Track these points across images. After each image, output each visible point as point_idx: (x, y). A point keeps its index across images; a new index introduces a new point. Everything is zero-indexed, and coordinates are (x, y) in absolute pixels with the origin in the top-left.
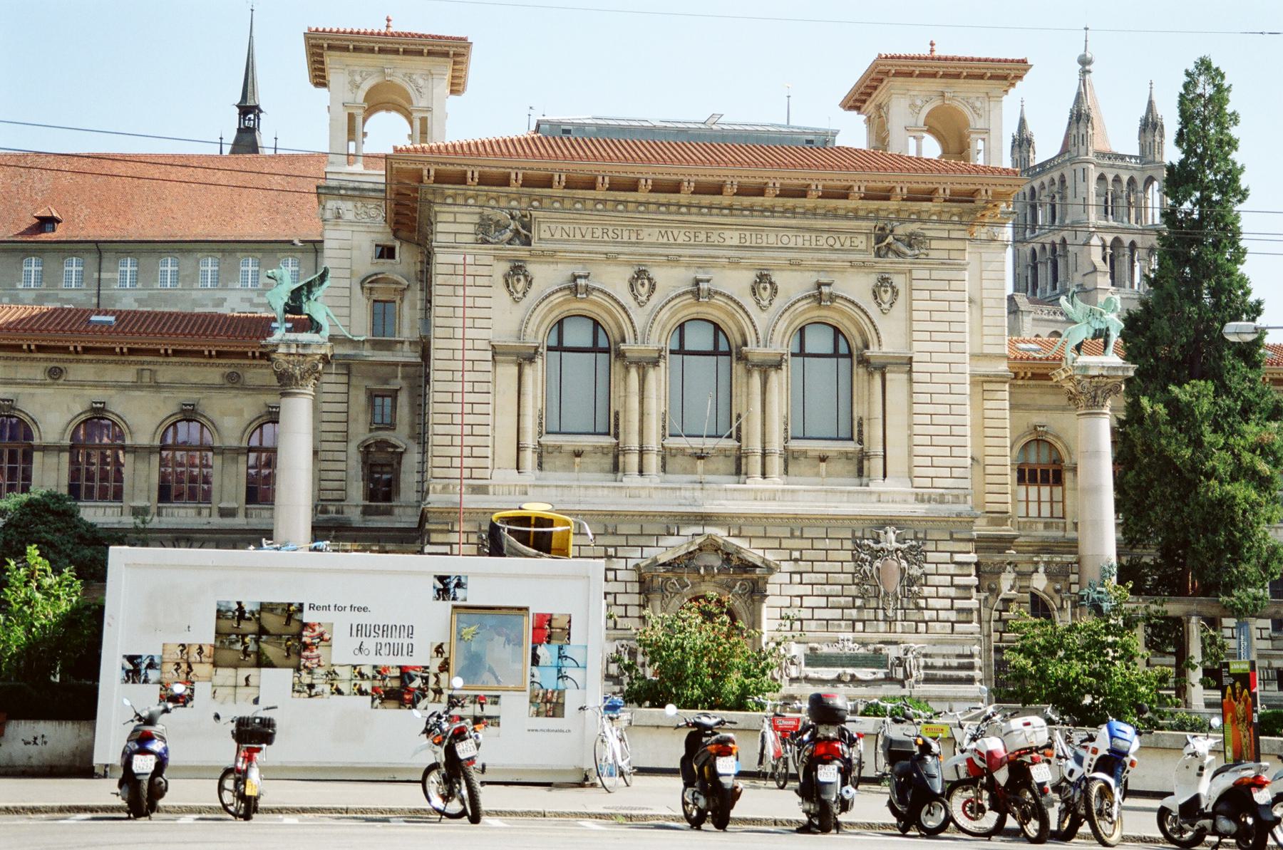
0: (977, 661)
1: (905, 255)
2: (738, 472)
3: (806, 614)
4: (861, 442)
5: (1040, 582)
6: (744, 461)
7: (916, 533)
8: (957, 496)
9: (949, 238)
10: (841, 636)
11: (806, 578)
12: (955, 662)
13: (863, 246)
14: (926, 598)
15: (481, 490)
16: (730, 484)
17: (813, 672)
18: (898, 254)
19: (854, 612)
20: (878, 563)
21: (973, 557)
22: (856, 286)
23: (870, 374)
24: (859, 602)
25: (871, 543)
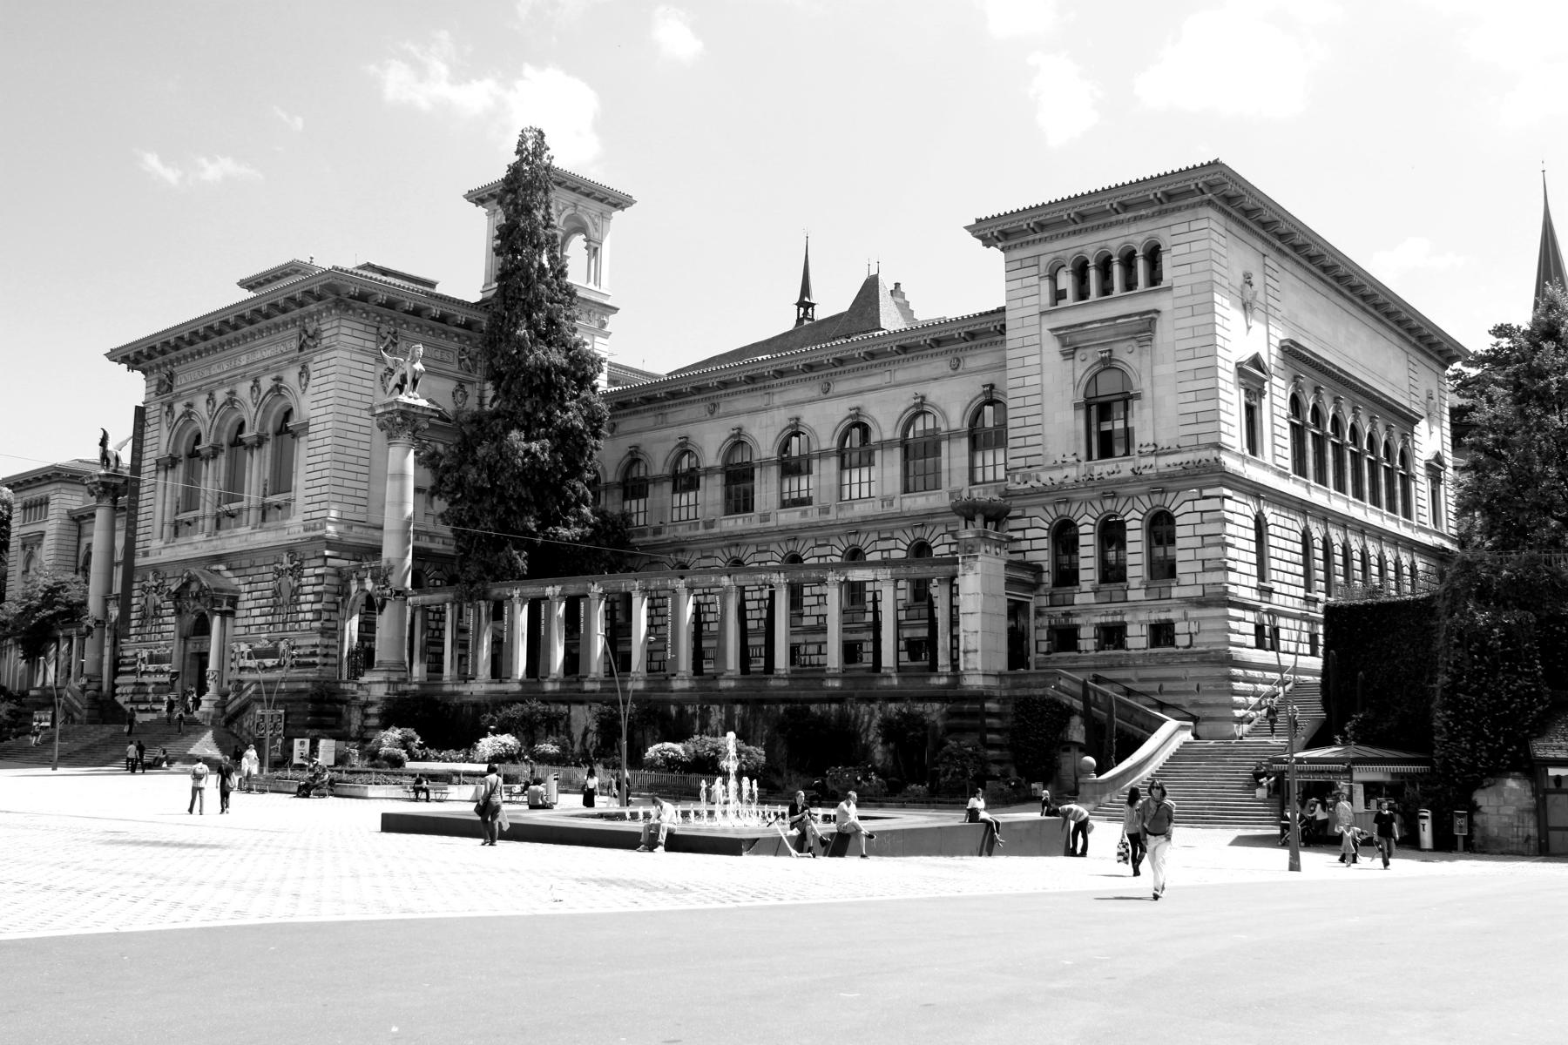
3: (251, 621)
5: (369, 585)
11: (255, 594)
12: (308, 651)
15: (146, 554)
17: (249, 663)
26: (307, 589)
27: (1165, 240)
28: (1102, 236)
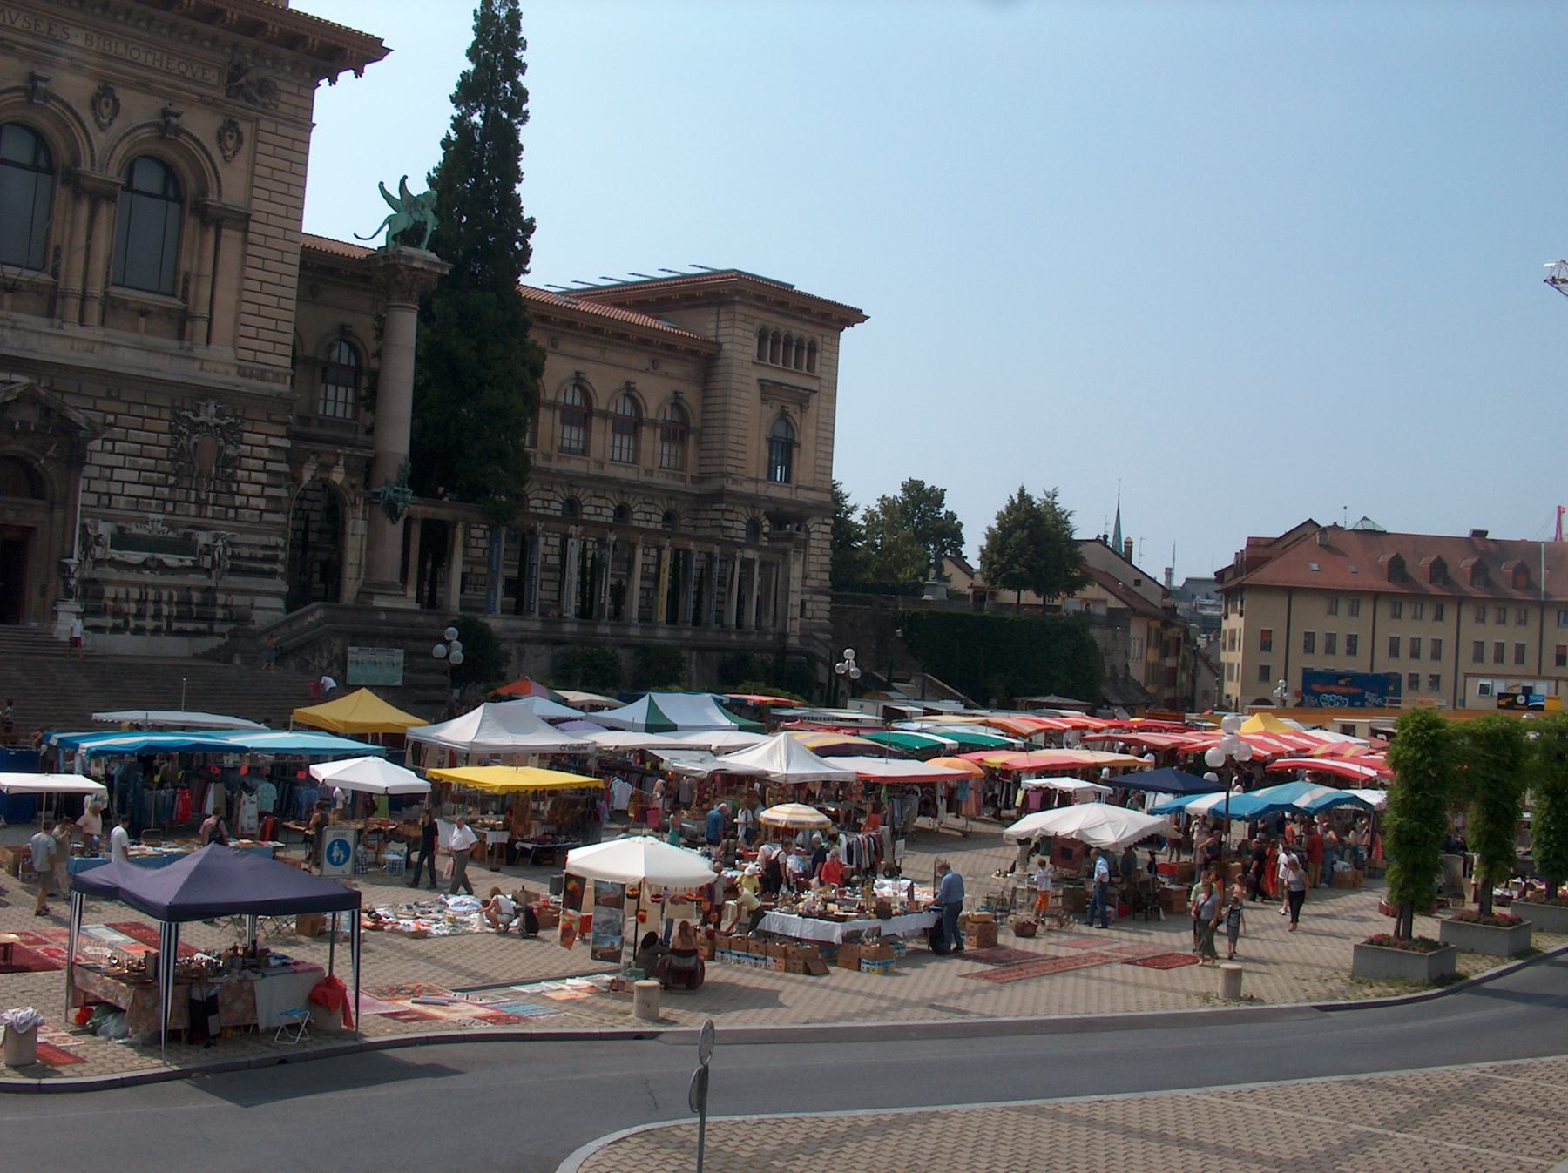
0: (282, 555)
1: (254, 101)
2: (50, 313)
3: (116, 488)
4: (185, 299)
5: (338, 476)
6: (59, 301)
7: (235, 410)
8: (277, 374)
9: (298, 95)
10: (151, 516)
12: (260, 553)
13: (214, 81)
14: (238, 482)
16: (41, 323)
17: (116, 554)
18: (249, 98)
19: (166, 491)
20: (195, 438)
21: (286, 443)
22: (201, 125)
23: (205, 224)
24: (172, 480)
25: (190, 414)
26: (251, 463)
27: (819, 339)
28: (790, 323)
